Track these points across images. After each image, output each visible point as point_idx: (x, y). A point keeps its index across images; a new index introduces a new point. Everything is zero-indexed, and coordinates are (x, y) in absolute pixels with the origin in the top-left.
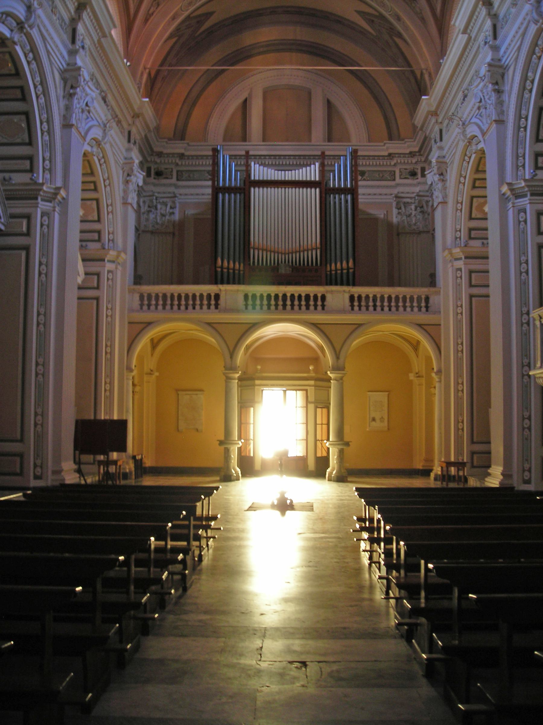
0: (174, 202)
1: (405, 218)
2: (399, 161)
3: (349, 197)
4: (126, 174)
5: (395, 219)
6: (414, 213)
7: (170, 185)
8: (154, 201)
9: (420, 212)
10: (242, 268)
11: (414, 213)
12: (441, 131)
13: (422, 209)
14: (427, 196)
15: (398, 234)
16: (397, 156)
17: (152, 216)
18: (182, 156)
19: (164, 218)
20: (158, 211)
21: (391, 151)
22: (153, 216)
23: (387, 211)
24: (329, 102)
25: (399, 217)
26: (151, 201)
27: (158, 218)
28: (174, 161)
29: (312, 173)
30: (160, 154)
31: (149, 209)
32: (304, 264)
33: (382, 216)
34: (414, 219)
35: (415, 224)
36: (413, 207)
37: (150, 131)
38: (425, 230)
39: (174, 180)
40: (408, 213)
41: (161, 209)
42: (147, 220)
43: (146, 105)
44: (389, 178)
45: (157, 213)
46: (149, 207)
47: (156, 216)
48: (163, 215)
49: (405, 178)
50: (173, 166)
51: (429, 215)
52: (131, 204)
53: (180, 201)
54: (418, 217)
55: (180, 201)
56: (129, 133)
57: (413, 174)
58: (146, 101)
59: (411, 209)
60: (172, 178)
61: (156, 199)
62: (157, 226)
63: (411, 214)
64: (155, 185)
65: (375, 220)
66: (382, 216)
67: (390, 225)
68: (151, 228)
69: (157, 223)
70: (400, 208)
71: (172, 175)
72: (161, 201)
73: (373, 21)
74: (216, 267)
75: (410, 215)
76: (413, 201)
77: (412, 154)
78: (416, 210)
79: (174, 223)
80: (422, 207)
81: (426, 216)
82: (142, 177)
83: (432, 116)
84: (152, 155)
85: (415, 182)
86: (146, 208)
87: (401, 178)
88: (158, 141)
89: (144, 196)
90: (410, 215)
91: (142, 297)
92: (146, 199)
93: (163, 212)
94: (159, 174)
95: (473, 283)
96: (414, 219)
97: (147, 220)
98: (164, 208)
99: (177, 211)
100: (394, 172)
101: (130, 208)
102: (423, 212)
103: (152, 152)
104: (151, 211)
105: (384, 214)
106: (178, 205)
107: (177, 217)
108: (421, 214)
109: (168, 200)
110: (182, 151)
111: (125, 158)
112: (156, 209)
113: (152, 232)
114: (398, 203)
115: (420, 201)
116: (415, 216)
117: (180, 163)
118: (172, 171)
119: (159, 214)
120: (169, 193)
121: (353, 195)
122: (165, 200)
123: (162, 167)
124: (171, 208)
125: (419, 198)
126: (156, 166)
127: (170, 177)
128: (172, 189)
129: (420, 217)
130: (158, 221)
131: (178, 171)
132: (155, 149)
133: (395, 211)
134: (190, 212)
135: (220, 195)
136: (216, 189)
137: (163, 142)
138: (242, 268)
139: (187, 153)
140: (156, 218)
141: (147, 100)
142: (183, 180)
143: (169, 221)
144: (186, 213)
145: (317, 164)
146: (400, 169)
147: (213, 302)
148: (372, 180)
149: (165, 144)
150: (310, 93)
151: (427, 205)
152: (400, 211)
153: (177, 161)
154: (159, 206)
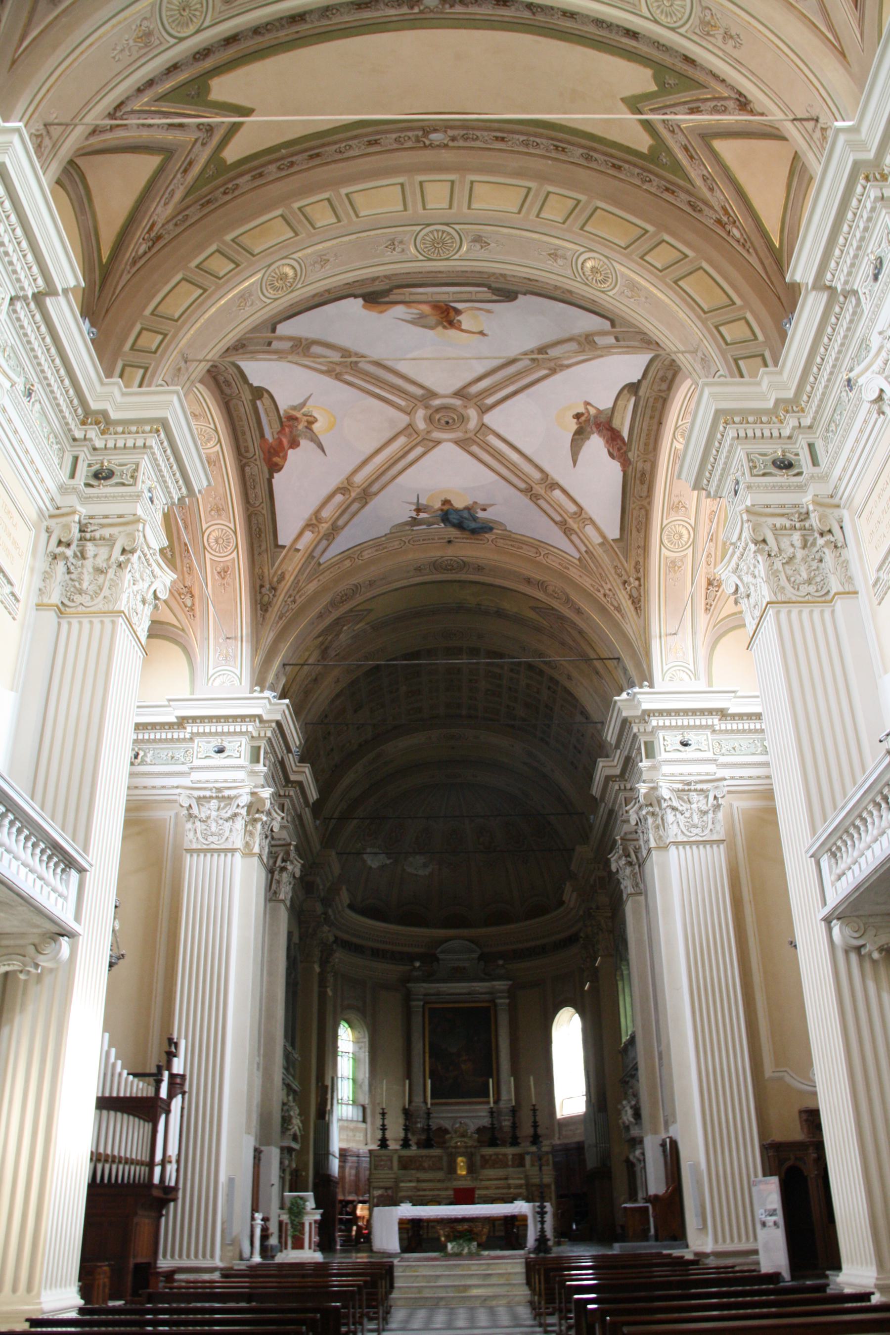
0: (132, 537)
1: (778, 565)
6: (800, 553)
26: (67, 527)
41: (95, 556)
49: (764, 475)
59: (793, 545)
64: (86, 500)
78: (804, 547)
83: (867, 179)
92: (52, 523)
93: (100, 562)
94: (101, 475)
98: (103, 552)
112: (84, 557)
116: (804, 560)
119: (91, 570)
124: (124, 551)
127: (131, 481)
130: (85, 585)
132: (94, 406)
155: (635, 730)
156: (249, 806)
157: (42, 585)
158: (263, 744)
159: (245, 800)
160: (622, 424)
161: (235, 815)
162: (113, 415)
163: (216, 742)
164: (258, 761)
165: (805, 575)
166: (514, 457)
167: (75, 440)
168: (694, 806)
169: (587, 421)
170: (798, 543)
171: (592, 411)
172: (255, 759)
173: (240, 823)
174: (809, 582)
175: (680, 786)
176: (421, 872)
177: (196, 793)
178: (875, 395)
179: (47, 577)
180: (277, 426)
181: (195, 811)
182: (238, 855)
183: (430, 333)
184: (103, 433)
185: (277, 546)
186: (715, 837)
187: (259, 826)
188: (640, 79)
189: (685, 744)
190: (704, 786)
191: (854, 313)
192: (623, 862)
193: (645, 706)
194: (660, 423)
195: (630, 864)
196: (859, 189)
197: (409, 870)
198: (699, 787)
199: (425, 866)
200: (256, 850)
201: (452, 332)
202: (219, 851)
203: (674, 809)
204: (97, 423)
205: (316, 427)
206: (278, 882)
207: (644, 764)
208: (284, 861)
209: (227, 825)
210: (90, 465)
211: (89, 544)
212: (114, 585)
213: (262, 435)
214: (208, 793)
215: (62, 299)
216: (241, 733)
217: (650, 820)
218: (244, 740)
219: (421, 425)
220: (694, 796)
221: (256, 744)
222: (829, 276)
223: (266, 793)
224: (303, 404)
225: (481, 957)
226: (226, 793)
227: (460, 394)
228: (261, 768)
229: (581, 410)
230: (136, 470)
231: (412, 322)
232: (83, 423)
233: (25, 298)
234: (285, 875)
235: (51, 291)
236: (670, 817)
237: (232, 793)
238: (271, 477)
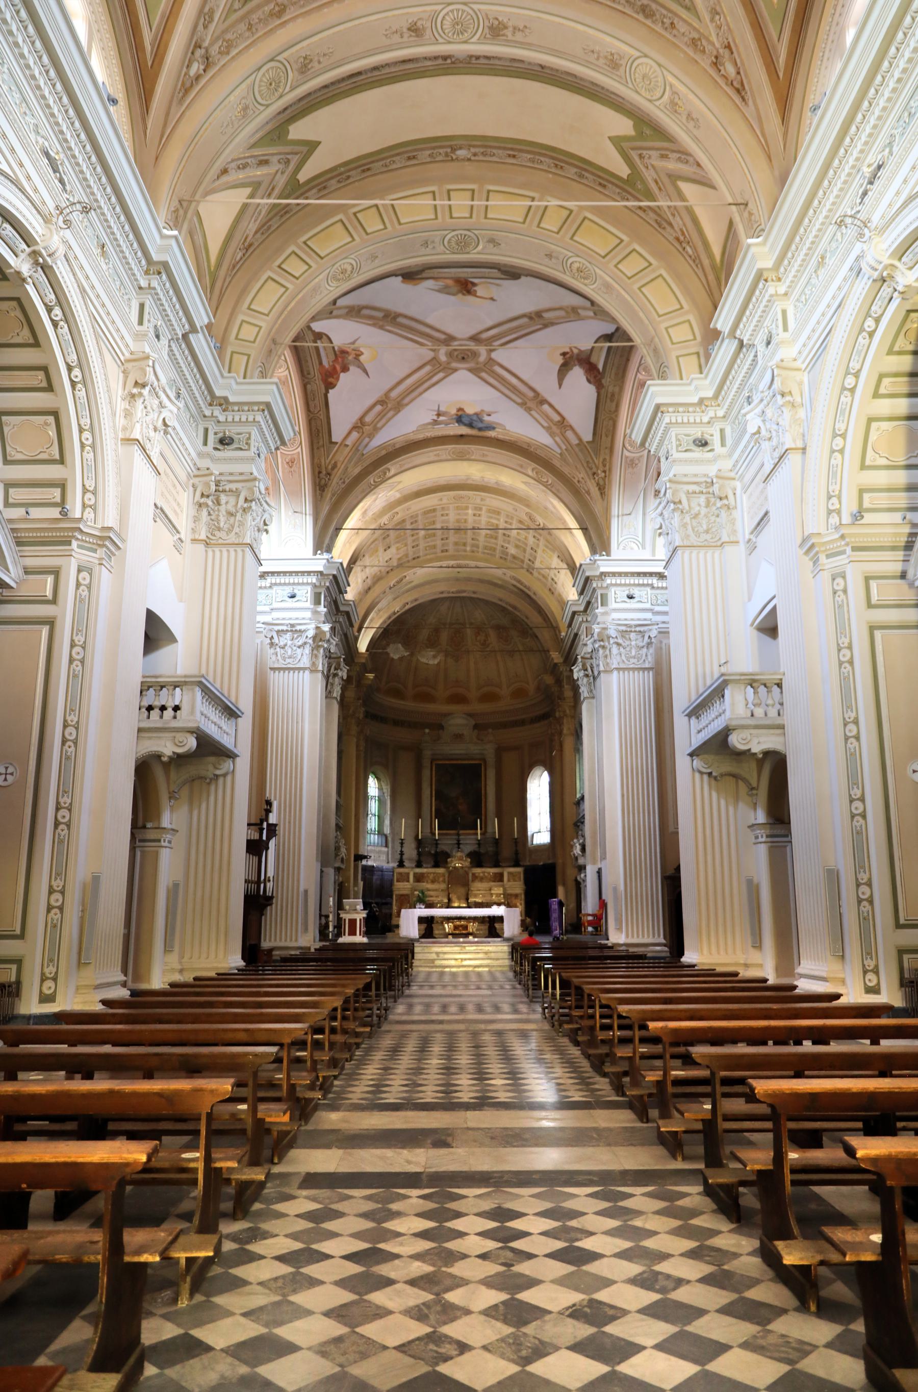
1: (687, 519)
4: (130, 382)
6: (704, 511)
16: (671, 409)
19: (232, 519)
26: (207, 485)
34: (704, 522)
78: (707, 506)
90: (696, 516)
92: (196, 480)
93: (230, 507)
95: (874, 599)
96: (704, 522)
98: (232, 500)
112: (219, 504)
116: (706, 516)
124: (246, 500)
130: (222, 525)
146: (677, 435)
155: (594, 585)
156: (314, 638)
157: (193, 525)
158: (323, 591)
159: (311, 633)
160: (598, 360)
161: (305, 643)
162: (232, 399)
163: (288, 590)
164: (319, 603)
165: (705, 527)
166: (514, 381)
168: (633, 643)
169: (571, 357)
170: (703, 504)
171: (575, 351)
172: (317, 602)
173: (307, 650)
174: (707, 532)
175: (624, 628)
176: (431, 662)
177: (276, 628)
179: (196, 519)
180: (332, 357)
181: (276, 640)
182: (307, 672)
183: (452, 298)
184: (224, 411)
185: (331, 442)
186: (647, 665)
187: (322, 651)
188: (624, 126)
189: (631, 597)
190: (642, 629)
192: (582, 674)
193: (603, 569)
194: (628, 360)
195: (587, 676)
197: (424, 660)
198: (638, 629)
199: (434, 657)
200: (320, 668)
201: (470, 298)
202: (294, 669)
203: (618, 644)
204: (221, 405)
205: (362, 358)
206: (332, 684)
207: (600, 610)
208: (336, 669)
209: (299, 651)
210: (216, 434)
212: (241, 524)
213: (321, 363)
214: (285, 628)
215: (200, 335)
216: (308, 584)
217: (601, 651)
218: (309, 588)
219: (443, 358)
220: (633, 635)
221: (318, 590)
223: (326, 628)
224: (353, 343)
225: (476, 727)
226: (298, 628)
227: (475, 338)
228: (322, 609)
229: (567, 350)
230: (249, 438)
231: (439, 291)
232: (210, 405)
233: (178, 339)
234: (337, 679)
235: (193, 329)
236: (615, 650)
237: (302, 628)
238: (327, 392)
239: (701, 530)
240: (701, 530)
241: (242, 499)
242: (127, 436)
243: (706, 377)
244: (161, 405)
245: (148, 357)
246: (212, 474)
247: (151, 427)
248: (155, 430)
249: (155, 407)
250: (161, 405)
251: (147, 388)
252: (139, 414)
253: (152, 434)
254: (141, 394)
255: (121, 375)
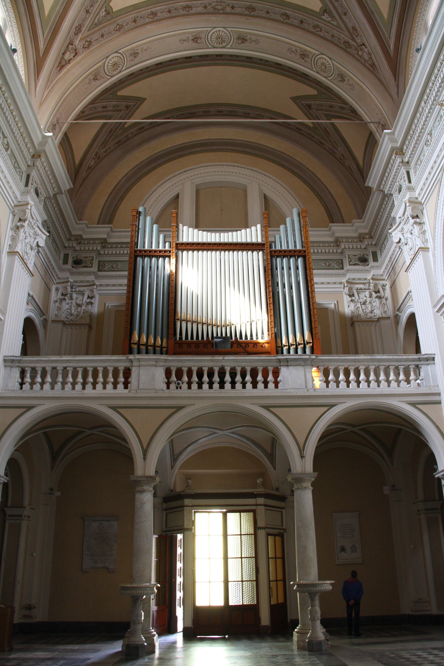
0: (92, 291)
1: (359, 305)
2: (347, 247)
3: (300, 260)
4: (17, 218)
5: (348, 308)
6: (368, 300)
7: (90, 274)
8: (69, 288)
9: (376, 297)
10: (164, 344)
11: (368, 300)
12: (408, 173)
13: (378, 294)
14: (384, 280)
15: (353, 324)
17: (65, 306)
18: (104, 243)
19: (79, 309)
20: (74, 302)
21: (337, 235)
22: (67, 306)
23: (337, 301)
24: (265, 197)
25: (352, 305)
26: (66, 288)
27: (73, 308)
28: (95, 248)
29: (253, 234)
30: (79, 239)
31: (62, 297)
32: (246, 336)
33: (333, 306)
35: (372, 312)
36: (367, 293)
37: (60, 192)
38: (384, 315)
39: (95, 268)
40: (362, 300)
41: (77, 298)
42: (59, 309)
43: (50, 140)
44: (337, 267)
45: (71, 303)
46: (62, 294)
47: (71, 306)
48: (79, 305)
49: (355, 265)
50: (94, 255)
51: (386, 300)
52: (18, 252)
53: (101, 292)
54: (374, 304)
55: (101, 292)
56: (28, 176)
57: (363, 260)
58: (49, 137)
59: (366, 296)
60: (92, 267)
61: (72, 288)
62: (72, 318)
63: (366, 301)
64: (72, 273)
65: (325, 310)
66: (333, 306)
67: (342, 317)
68: (63, 317)
69: (71, 315)
70: (353, 295)
71: (92, 264)
72: (78, 290)
73: (309, 106)
74: (130, 344)
75: (364, 303)
76: (367, 286)
77: (361, 238)
78: (371, 296)
79: (91, 315)
80: (379, 292)
81: (384, 300)
82: (44, 237)
84: (69, 240)
85: (367, 268)
86: (59, 296)
87: (350, 265)
88: (77, 223)
89: (57, 283)
90: (364, 303)
91: (23, 373)
92: (59, 286)
93: (79, 302)
94: (77, 262)
97: (59, 309)
98: (80, 297)
99: (96, 301)
100: (342, 260)
101: (17, 262)
102: (380, 298)
103: (71, 237)
104: (65, 299)
105: (335, 304)
106: (97, 297)
107: (95, 309)
108: (377, 299)
109: (85, 288)
110: (105, 236)
111: (19, 202)
112: (72, 299)
113: (64, 323)
114: (350, 289)
115: (375, 285)
117: (102, 252)
118: (93, 260)
119: (75, 305)
120: (88, 281)
121: (304, 257)
122: (82, 289)
123: (82, 256)
124: (89, 297)
125: (374, 282)
126: (75, 254)
127: (91, 265)
128: (91, 278)
129: (376, 303)
130: (73, 311)
131: (99, 262)
133: (346, 299)
134: (110, 304)
135: (139, 260)
136: (135, 251)
137: (83, 224)
138: (164, 344)
139: (110, 241)
140: (71, 309)
141: (51, 134)
142: (105, 271)
143: (85, 312)
144: (107, 305)
145: (259, 226)
146: (348, 256)
147: (121, 379)
148: (317, 269)
149: (84, 226)
150: (245, 191)
151: (384, 290)
152: (353, 298)
153: (99, 248)
154: (75, 296)
167: (65, 247)
170: (368, 296)
178: (398, 240)
191: (391, 206)
196: (393, 157)
210: (73, 258)
211: (74, 293)
222: (382, 186)
239: (368, 311)
240: (368, 311)
241: (86, 296)
242: (12, 251)
243: (363, 222)
244: (36, 234)
245: (28, 204)
246: (68, 282)
247: (29, 247)
248: (32, 248)
249: (31, 234)
250: (36, 234)
251: (27, 222)
252: (21, 238)
253: (29, 251)
254: (23, 226)
255: (11, 215)
